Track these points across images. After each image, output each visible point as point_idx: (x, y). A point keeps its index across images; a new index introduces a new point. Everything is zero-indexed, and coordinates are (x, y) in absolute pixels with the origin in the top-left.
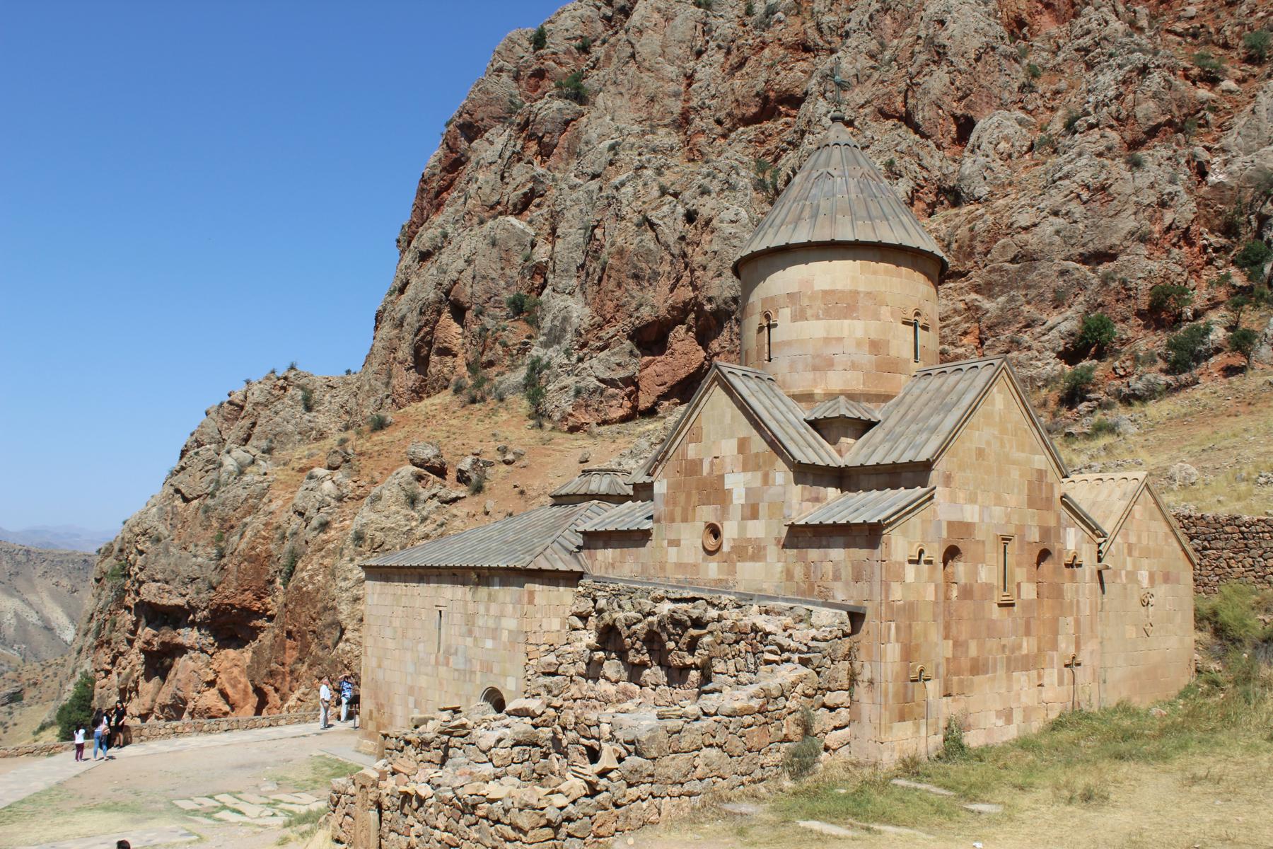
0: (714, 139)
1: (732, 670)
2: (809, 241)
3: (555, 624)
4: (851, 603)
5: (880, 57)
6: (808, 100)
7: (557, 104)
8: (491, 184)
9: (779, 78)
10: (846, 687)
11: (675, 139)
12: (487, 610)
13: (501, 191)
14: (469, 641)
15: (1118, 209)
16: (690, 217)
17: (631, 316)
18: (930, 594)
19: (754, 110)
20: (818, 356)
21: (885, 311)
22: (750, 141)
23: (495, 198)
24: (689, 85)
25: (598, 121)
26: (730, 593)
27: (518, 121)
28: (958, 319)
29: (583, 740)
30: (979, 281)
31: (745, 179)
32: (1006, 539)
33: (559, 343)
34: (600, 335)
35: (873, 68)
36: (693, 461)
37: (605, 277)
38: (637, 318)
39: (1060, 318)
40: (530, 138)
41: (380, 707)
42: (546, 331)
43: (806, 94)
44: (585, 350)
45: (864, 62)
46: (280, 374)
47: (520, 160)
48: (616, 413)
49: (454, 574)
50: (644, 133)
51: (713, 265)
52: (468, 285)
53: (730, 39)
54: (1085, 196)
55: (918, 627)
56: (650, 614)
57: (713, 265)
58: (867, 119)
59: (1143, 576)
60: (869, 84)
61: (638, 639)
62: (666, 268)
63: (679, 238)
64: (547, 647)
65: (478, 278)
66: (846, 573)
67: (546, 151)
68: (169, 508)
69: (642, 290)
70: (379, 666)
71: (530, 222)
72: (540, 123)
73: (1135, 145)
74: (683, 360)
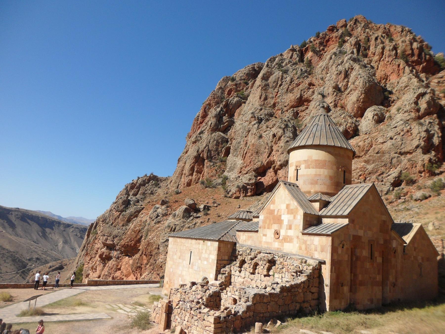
0: (284, 112)
1: (280, 277)
2: (312, 144)
3: (226, 258)
4: (320, 258)
9: (305, 93)
12: (206, 252)
14: (199, 261)
15: (414, 138)
16: (274, 136)
18: (346, 258)
24: (276, 95)
26: (281, 252)
27: (224, 103)
28: (358, 170)
30: (365, 159)
33: (233, 171)
35: (334, 91)
37: (248, 152)
39: (393, 172)
41: (170, 280)
42: (229, 167)
43: (313, 99)
44: (240, 174)
45: (331, 90)
46: (148, 175)
48: (249, 194)
51: (280, 150)
54: (402, 134)
58: (332, 107)
59: (419, 258)
62: (267, 150)
63: (271, 142)
66: (319, 249)
68: (111, 214)
69: (258, 157)
70: (171, 267)
73: (420, 118)
74: (271, 178)
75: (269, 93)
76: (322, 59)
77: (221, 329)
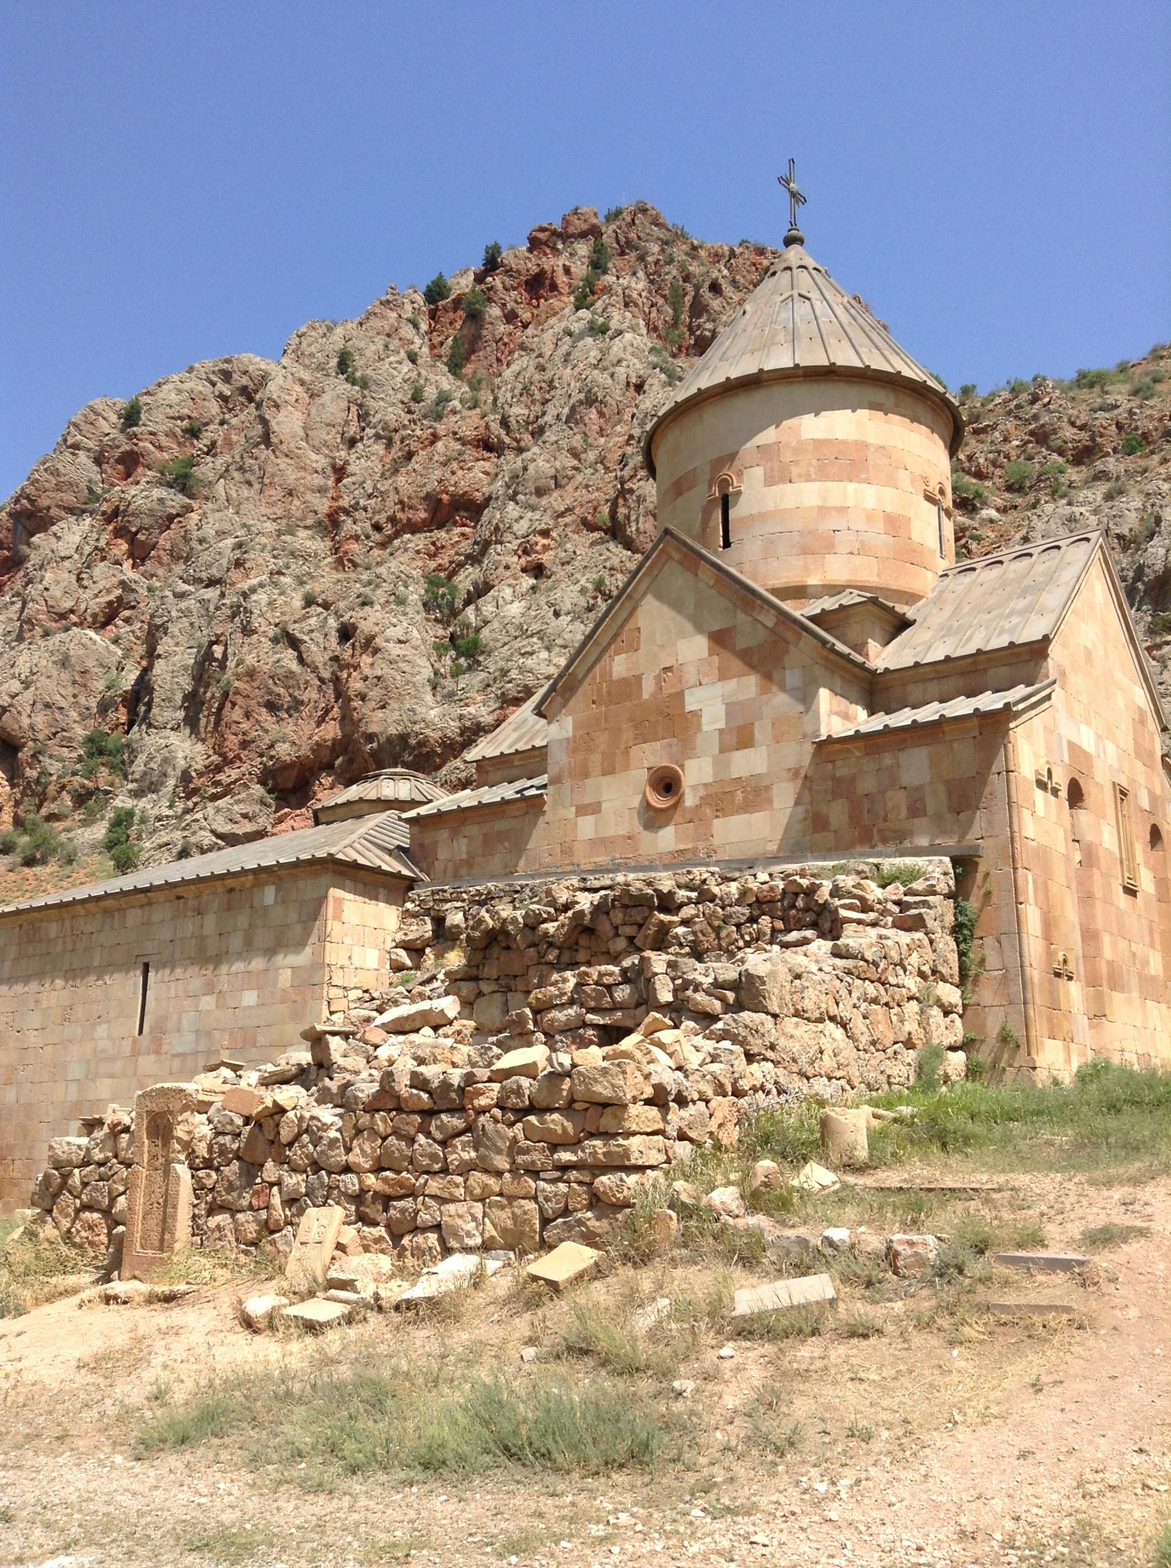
5: (583, 456)
6: (493, 504)
7: (158, 492)
8: (62, 585)
10: (957, 979)
11: (320, 545)
13: (76, 595)
14: (208, 1002)
16: (346, 633)
17: (261, 755)
18: (1059, 842)
19: (423, 515)
20: (810, 532)
21: (902, 475)
22: (418, 552)
23: (68, 604)
24: (339, 480)
25: (217, 515)
26: (707, 865)
29: (590, 1016)
31: (415, 594)
32: (1123, 793)
34: (218, 777)
36: (624, 681)
37: (228, 705)
38: (272, 758)
40: (118, 533)
47: (103, 559)
49: (179, 898)
50: (280, 533)
52: (24, 714)
53: (393, 425)
55: (1054, 889)
56: (566, 907)
57: (375, 694)
58: (569, 529)
60: (570, 488)
61: (551, 944)
62: (315, 695)
64: (359, 993)
65: (39, 706)
67: (139, 554)
71: (116, 641)
72: (133, 515)
75: (304, 469)
76: (511, 352)
77: (660, 1138)
